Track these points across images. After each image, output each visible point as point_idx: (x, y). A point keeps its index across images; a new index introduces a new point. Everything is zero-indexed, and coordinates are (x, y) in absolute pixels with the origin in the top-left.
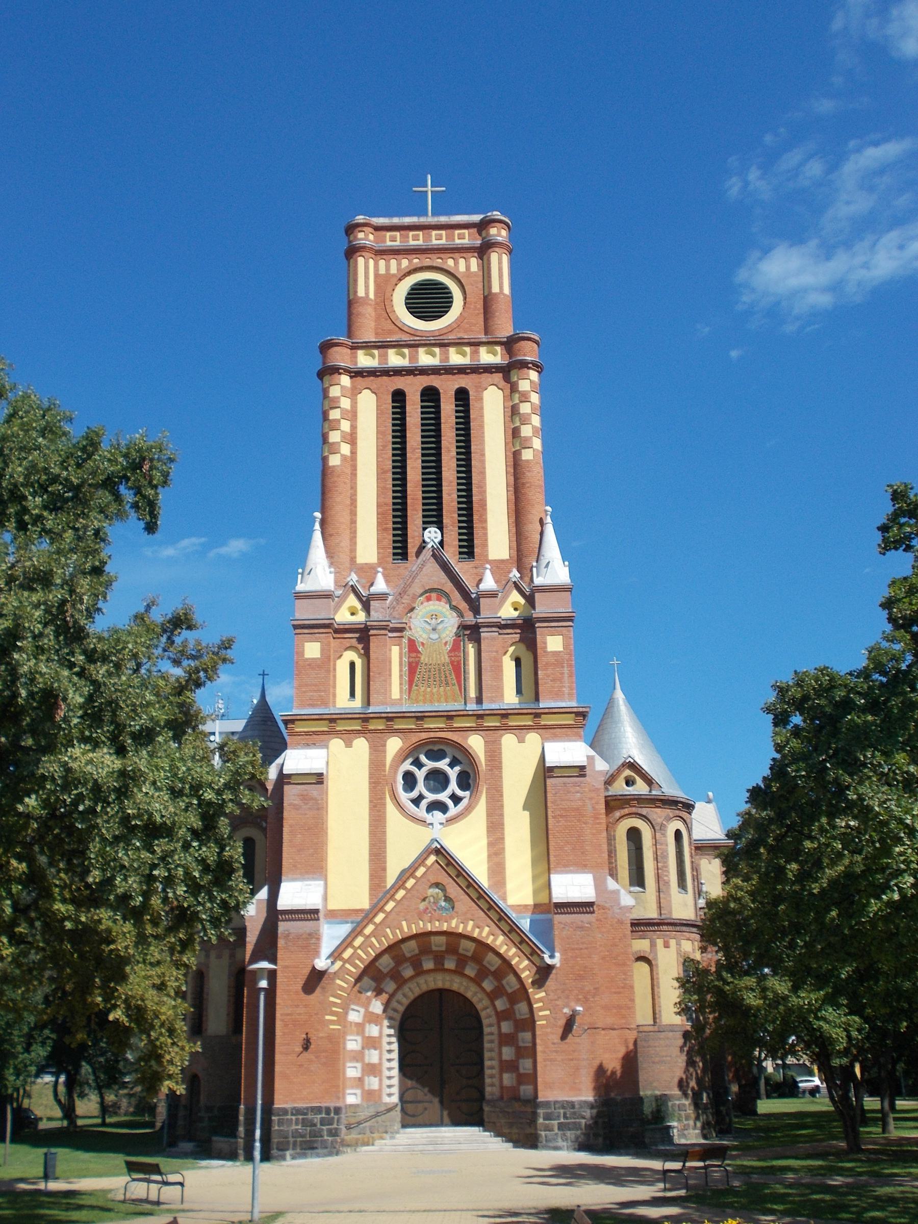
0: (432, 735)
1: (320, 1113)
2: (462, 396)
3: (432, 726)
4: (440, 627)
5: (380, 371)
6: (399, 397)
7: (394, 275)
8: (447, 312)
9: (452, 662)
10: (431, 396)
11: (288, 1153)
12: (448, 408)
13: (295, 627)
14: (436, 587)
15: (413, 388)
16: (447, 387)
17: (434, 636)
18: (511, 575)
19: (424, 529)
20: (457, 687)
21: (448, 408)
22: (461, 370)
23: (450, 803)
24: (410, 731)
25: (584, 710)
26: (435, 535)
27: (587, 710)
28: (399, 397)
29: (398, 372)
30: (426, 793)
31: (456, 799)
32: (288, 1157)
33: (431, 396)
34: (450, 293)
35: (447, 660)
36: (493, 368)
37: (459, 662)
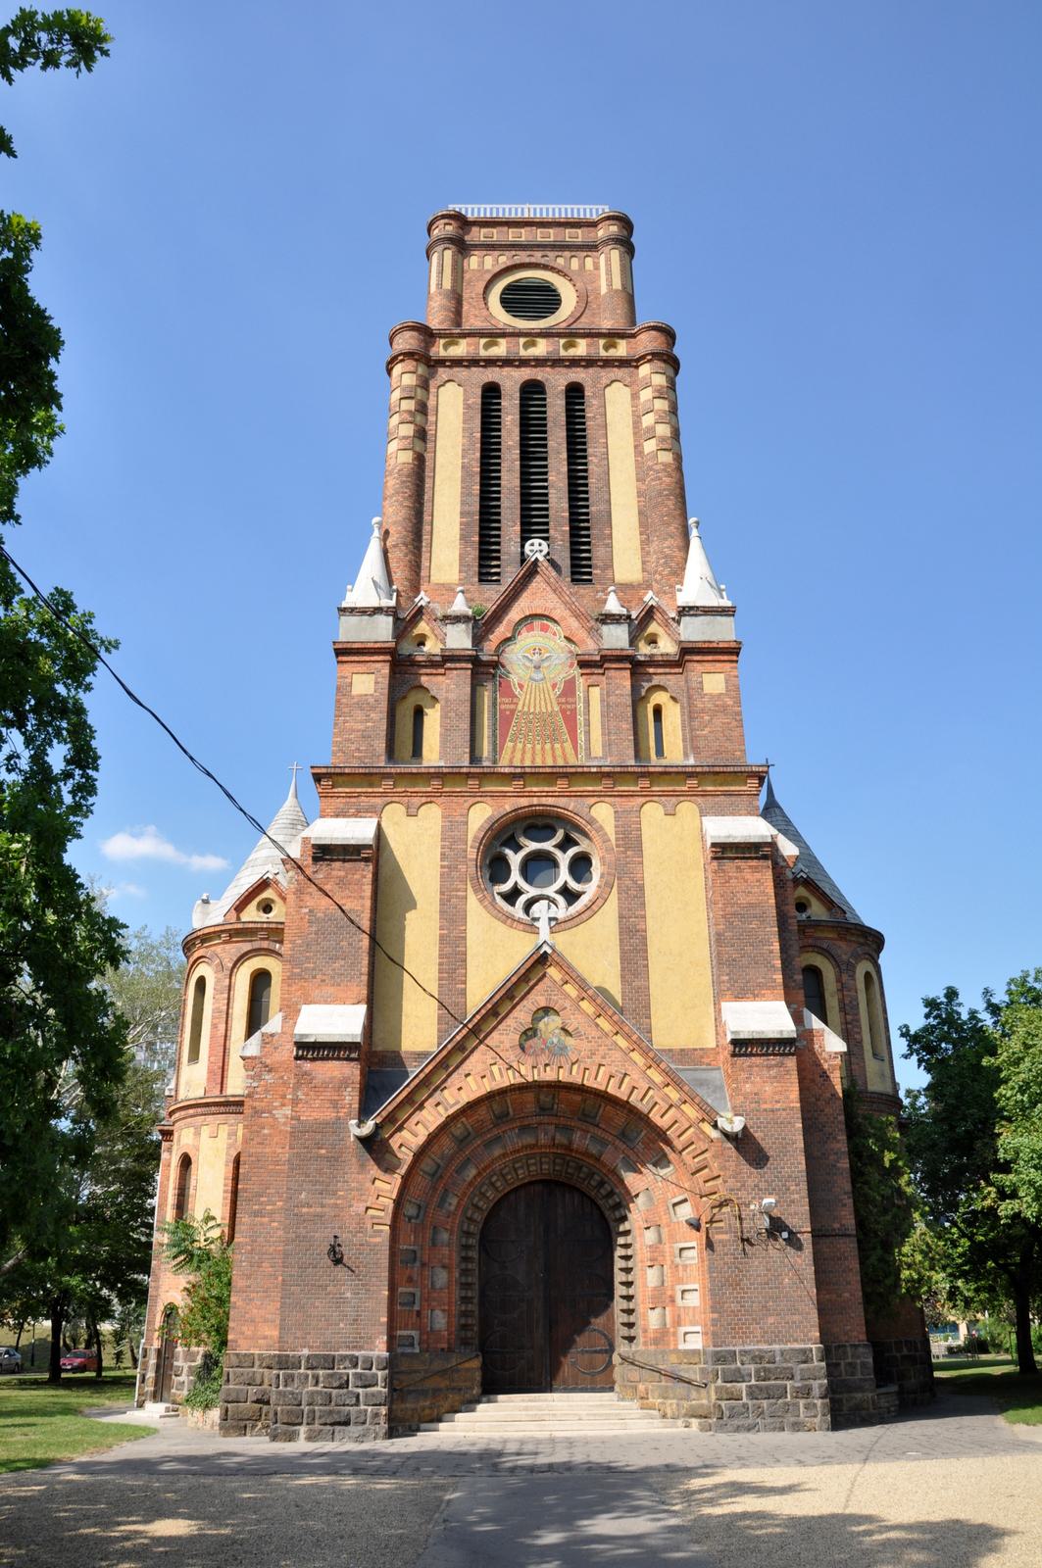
0: (535, 801)
1: (355, 1366)
2: (575, 393)
3: (535, 789)
4: (546, 664)
5: (467, 360)
6: (491, 392)
7: (488, 271)
8: (554, 313)
9: (563, 711)
10: (532, 392)
11: (303, 1429)
12: (556, 408)
13: (339, 652)
14: (539, 612)
15: (511, 381)
16: (556, 382)
17: (538, 676)
18: (646, 599)
19: (524, 540)
20: (568, 745)
21: (556, 408)
22: (575, 362)
23: (560, 899)
24: (504, 795)
25: (761, 769)
26: (540, 548)
27: (765, 769)
28: (491, 392)
29: (490, 362)
30: (523, 884)
31: (570, 896)
32: (302, 1436)
33: (532, 392)
34: (559, 295)
35: (557, 708)
36: (616, 360)
37: (574, 711)
